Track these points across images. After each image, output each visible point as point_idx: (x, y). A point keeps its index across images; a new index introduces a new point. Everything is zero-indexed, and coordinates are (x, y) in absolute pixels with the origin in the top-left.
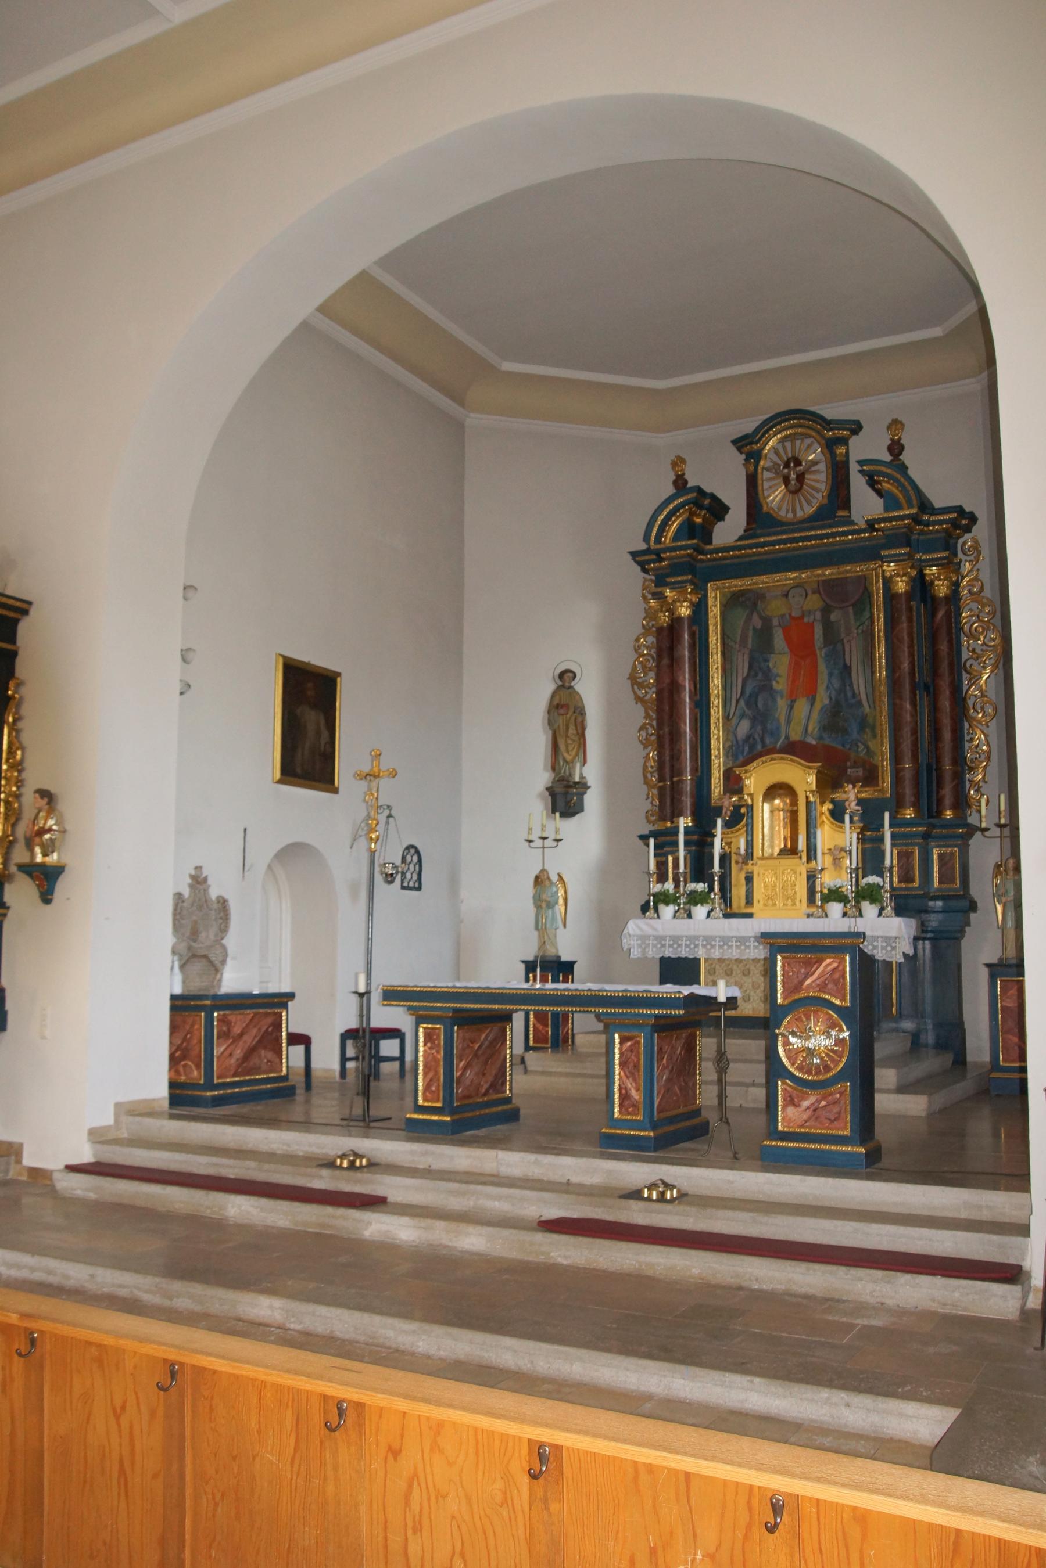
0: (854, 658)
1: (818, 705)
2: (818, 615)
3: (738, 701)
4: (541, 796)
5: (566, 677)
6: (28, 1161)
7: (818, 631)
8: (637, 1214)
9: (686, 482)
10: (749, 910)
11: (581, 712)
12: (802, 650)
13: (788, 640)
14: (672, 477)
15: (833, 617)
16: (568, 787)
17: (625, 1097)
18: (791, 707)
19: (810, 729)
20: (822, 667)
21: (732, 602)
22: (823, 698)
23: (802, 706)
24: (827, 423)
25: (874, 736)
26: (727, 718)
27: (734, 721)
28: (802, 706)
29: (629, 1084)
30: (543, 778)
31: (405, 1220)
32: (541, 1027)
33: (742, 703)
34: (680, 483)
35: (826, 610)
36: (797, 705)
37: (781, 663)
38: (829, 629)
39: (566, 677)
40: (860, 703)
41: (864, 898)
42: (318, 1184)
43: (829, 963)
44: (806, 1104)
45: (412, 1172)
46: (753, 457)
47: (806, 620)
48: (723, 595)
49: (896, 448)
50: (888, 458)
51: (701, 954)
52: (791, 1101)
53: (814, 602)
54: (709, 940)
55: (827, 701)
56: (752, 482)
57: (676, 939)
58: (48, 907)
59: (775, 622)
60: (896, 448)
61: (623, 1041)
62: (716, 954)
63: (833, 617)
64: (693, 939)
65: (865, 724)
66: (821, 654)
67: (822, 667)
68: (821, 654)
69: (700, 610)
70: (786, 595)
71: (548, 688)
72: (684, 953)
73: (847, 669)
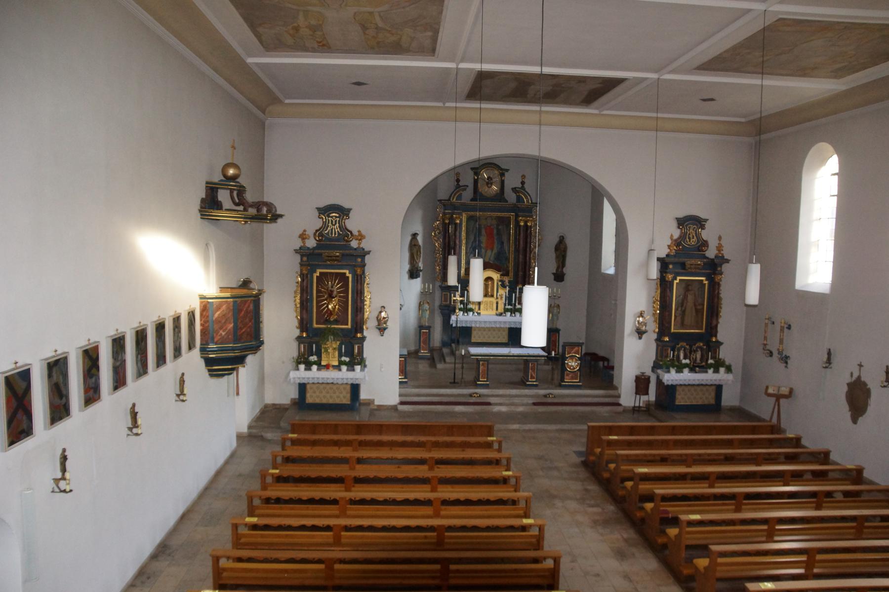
0: (505, 238)
1: (494, 252)
2: (495, 226)
3: (470, 249)
4: (408, 273)
5: (415, 235)
6: (376, 403)
7: (495, 231)
8: (549, 400)
9: (459, 181)
10: (479, 312)
11: (420, 246)
12: (490, 235)
13: (486, 232)
14: (456, 178)
15: (500, 227)
16: (418, 270)
17: (532, 376)
18: (486, 252)
19: (491, 259)
20: (495, 241)
21: (470, 219)
22: (495, 251)
23: (489, 252)
24: (502, 169)
25: (509, 262)
26: (466, 253)
27: (469, 254)
28: (489, 252)
29: (533, 373)
30: (407, 267)
31: (504, 407)
32: (424, 346)
33: (471, 249)
34: (458, 181)
35: (498, 225)
36: (488, 251)
37: (484, 239)
38: (498, 230)
39: (415, 235)
40: (506, 253)
41: (517, 311)
42: (472, 401)
43: (576, 348)
44: (570, 376)
45: (493, 396)
46: (476, 174)
47: (492, 227)
48: (467, 216)
49: (523, 183)
50: (520, 186)
51: (473, 325)
52: (567, 375)
53: (494, 222)
54: (476, 322)
55: (496, 251)
56: (476, 182)
57: (466, 322)
58: (382, 337)
59: (483, 226)
60: (523, 183)
61: (532, 364)
62: (478, 326)
63: (500, 227)
64: (471, 322)
65: (507, 259)
66: (496, 237)
67: (495, 241)
68: (496, 237)
69: (461, 221)
70: (486, 219)
71: (410, 238)
72: (468, 325)
73: (503, 243)
